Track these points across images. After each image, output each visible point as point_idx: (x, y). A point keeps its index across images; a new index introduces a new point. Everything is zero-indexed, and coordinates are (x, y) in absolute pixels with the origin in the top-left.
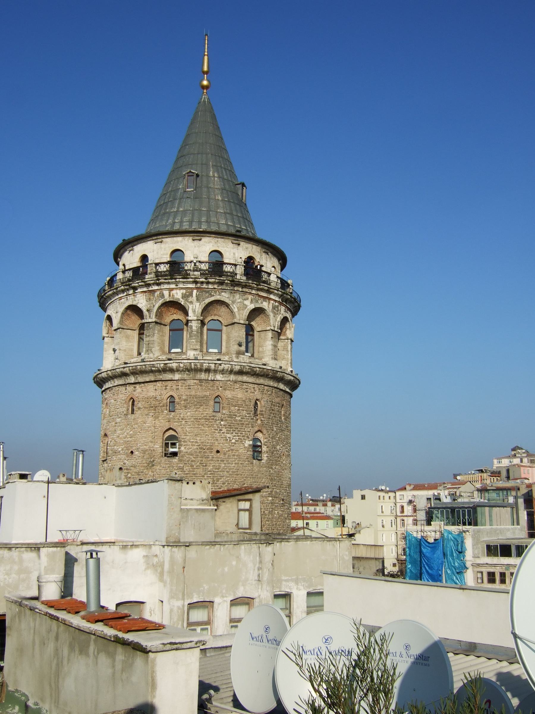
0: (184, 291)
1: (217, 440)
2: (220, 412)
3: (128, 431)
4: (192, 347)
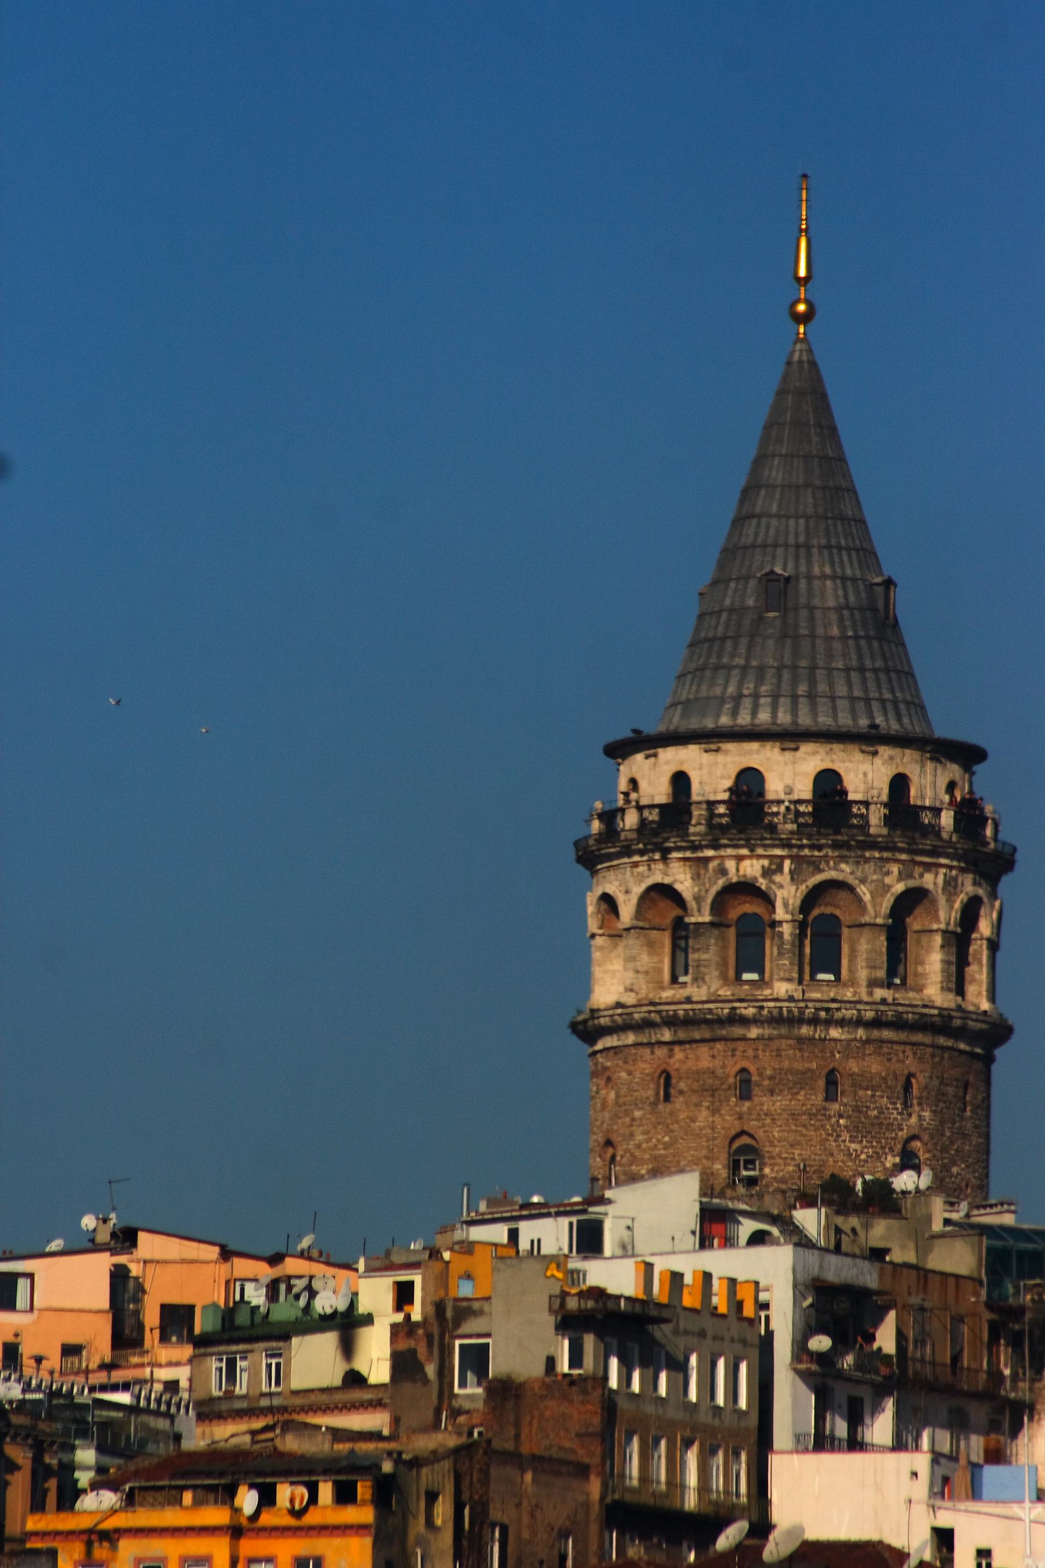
0: (766, 862)
1: (832, 1155)
2: (836, 1100)
3: (659, 1137)
4: (782, 974)
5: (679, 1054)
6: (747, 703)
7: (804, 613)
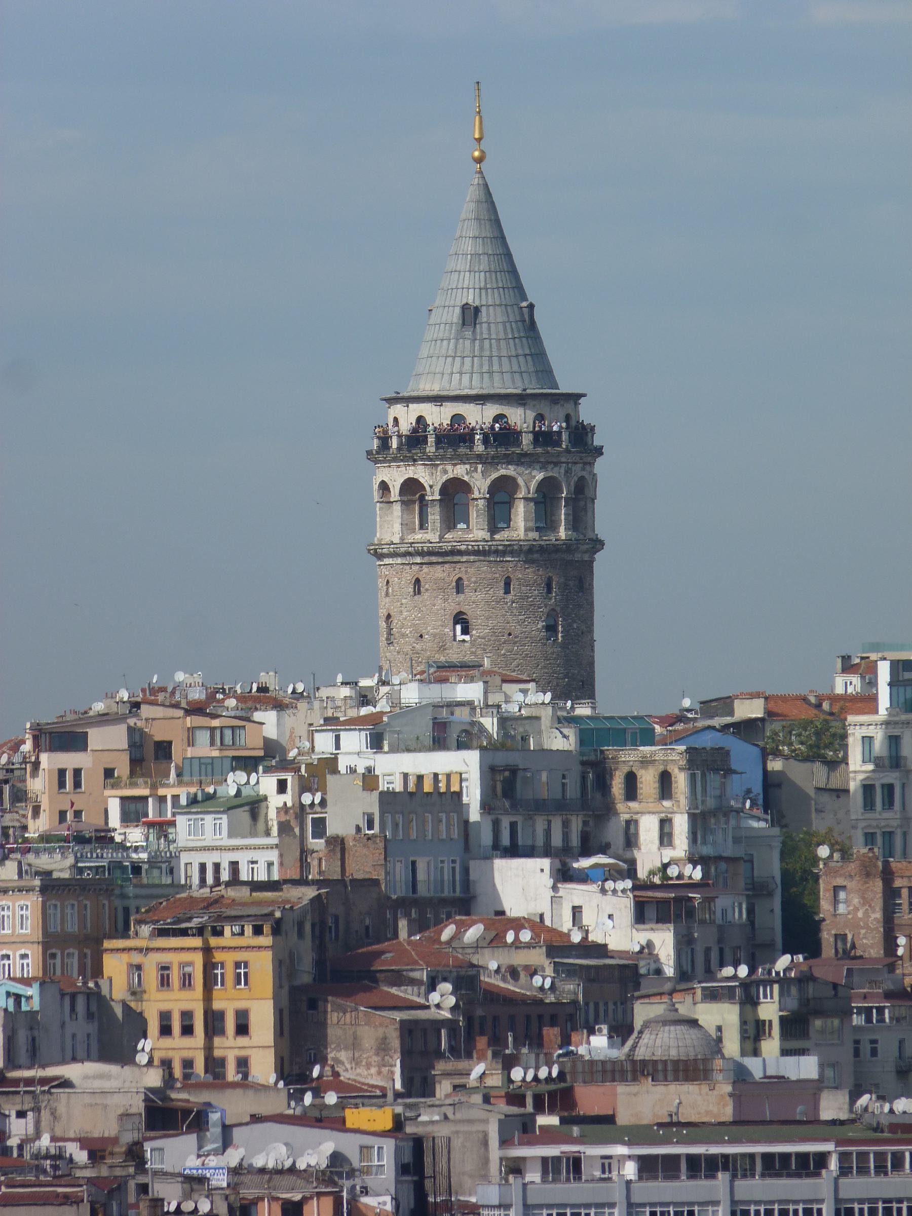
0: (468, 466)
1: (508, 623)
5: (425, 569)
6: (456, 377)
7: (485, 326)
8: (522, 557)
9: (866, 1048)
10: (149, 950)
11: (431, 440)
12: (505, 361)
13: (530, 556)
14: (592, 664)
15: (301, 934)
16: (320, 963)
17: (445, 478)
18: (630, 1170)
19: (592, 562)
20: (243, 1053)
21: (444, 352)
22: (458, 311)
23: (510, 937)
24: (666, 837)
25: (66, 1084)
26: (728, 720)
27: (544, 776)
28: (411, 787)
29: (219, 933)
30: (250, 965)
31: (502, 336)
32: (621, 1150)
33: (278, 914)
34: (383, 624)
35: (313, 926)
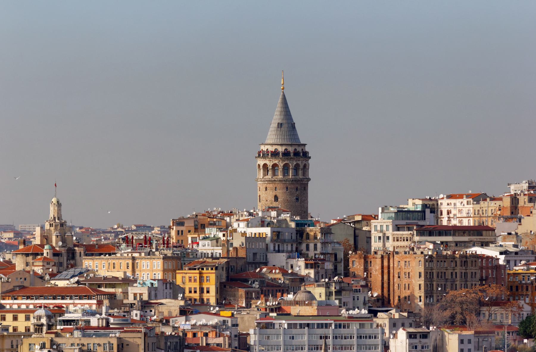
7: (283, 128)
8: (291, 182)
9: (356, 298)
10: (186, 273)
11: (270, 154)
12: (288, 136)
13: (292, 182)
14: (307, 208)
15: (223, 270)
16: (227, 277)
17: (273, 163)
18: (286, 326)
19: (307, 184)
20: (208, 297)
21: (273, 134)
22: (277, 124)
23: (274, 271)
24: (315, 248)
25: (162, 304)
26: (353, 220)
27: (287, 234)
28: (253, 236)
29: (203, 269)
30: (210, 277)
31: (287, 130)
32: (284, 322)
33: (217, 265)
34: (259, 198)
35: (226, 268)
